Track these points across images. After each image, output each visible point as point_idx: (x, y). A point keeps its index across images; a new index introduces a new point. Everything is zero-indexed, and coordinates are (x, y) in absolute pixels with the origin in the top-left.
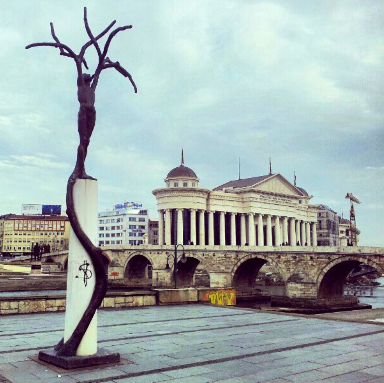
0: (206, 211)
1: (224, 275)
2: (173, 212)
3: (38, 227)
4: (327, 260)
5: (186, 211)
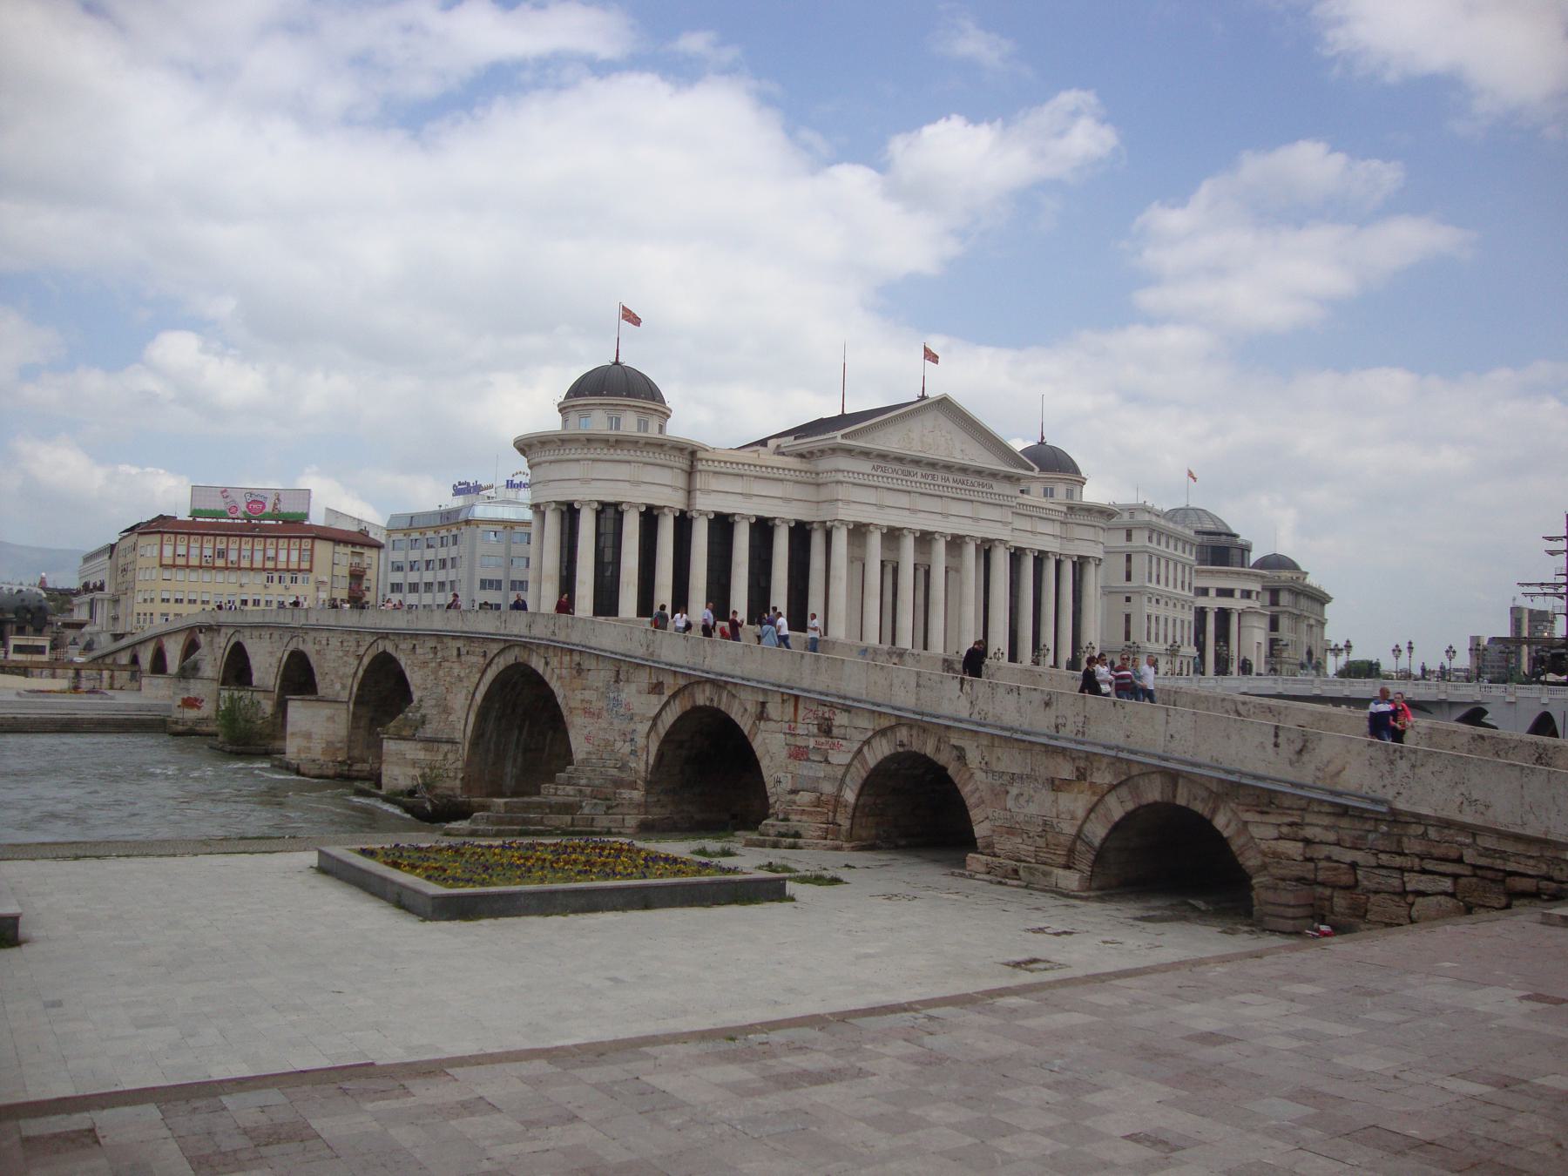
0: (683, 513)
1: (326, 711)
2: (570, 514)
3: (233, 556)
4: (481, 660)
5: (610, 512)
